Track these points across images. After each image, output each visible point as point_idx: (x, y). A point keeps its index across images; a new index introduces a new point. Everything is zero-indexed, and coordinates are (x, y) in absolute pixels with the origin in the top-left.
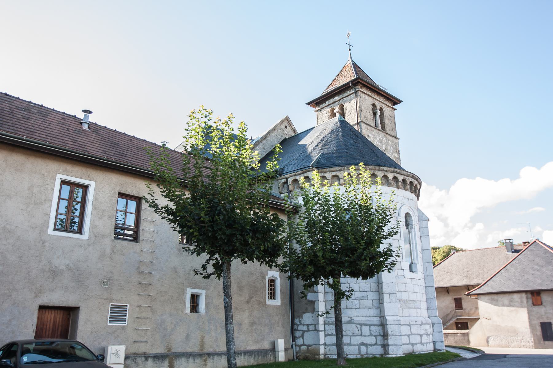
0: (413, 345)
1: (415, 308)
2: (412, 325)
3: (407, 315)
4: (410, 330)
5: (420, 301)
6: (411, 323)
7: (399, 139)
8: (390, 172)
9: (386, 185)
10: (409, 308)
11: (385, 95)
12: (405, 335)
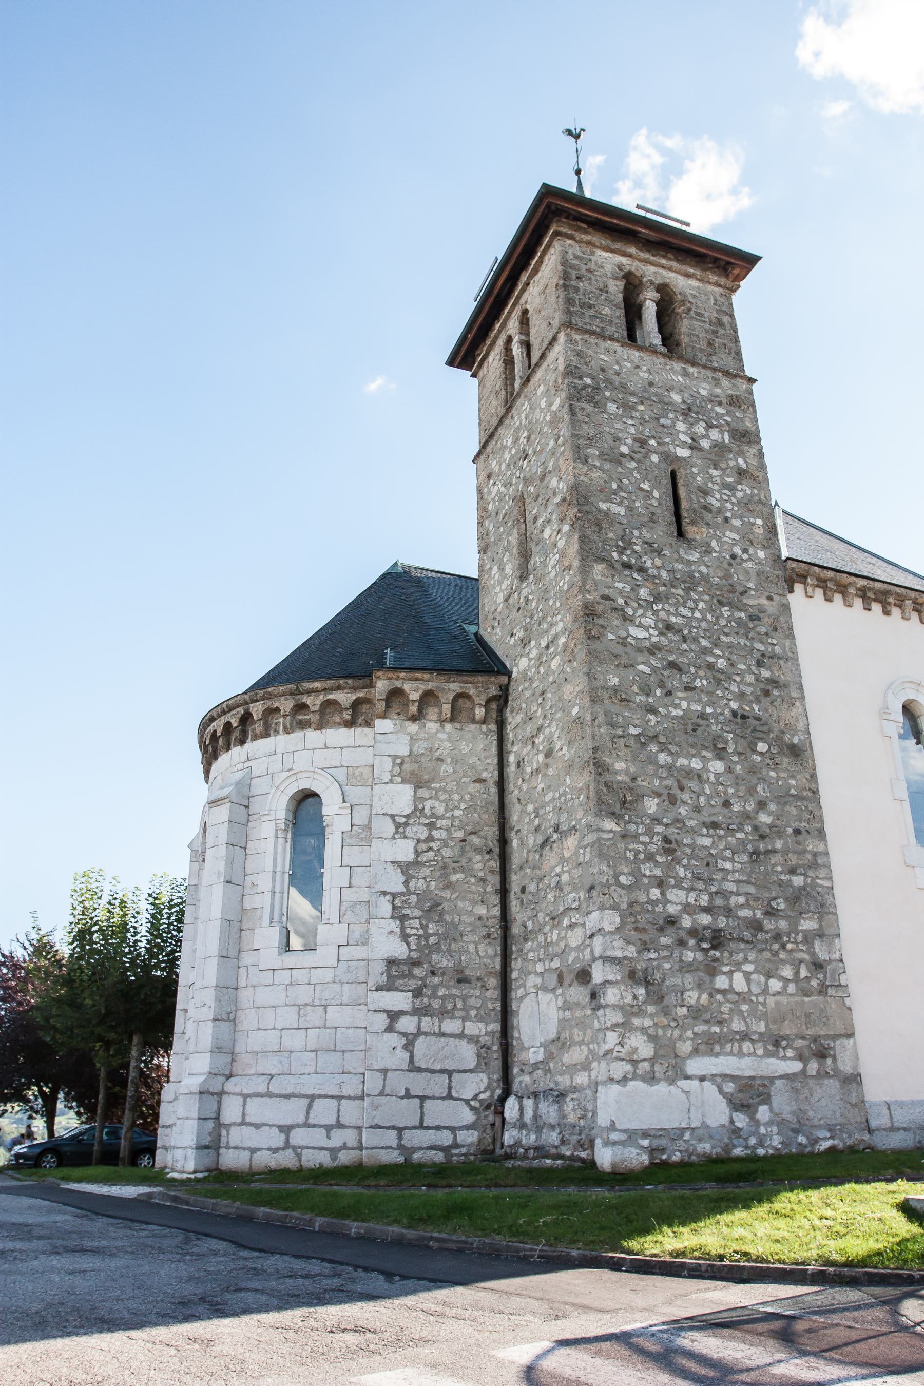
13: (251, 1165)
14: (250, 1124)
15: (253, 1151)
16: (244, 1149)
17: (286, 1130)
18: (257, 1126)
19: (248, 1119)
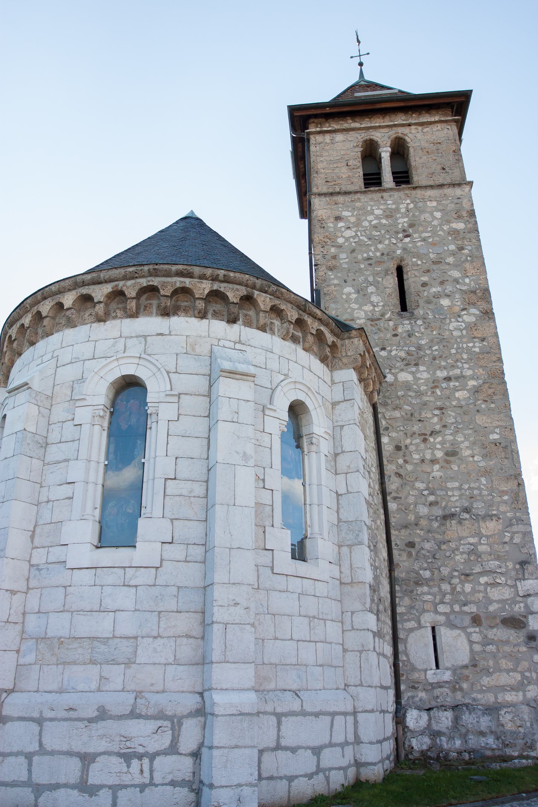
1: (93, 662)
2: (51, 720)
3: (55, 686)
4: (37, 738)
5: (136, 638)
6: (49, 714)
7: (471, 184)
8: (69, 290)
9: (67, 328)
10: (64, 663)
11: (402, 104)
13: (289, 796)
14: (286, 748)
15: (291, 779)
16: (281, 778)
17: (317, 751)
18: (294, 750)
19: (283, 743)
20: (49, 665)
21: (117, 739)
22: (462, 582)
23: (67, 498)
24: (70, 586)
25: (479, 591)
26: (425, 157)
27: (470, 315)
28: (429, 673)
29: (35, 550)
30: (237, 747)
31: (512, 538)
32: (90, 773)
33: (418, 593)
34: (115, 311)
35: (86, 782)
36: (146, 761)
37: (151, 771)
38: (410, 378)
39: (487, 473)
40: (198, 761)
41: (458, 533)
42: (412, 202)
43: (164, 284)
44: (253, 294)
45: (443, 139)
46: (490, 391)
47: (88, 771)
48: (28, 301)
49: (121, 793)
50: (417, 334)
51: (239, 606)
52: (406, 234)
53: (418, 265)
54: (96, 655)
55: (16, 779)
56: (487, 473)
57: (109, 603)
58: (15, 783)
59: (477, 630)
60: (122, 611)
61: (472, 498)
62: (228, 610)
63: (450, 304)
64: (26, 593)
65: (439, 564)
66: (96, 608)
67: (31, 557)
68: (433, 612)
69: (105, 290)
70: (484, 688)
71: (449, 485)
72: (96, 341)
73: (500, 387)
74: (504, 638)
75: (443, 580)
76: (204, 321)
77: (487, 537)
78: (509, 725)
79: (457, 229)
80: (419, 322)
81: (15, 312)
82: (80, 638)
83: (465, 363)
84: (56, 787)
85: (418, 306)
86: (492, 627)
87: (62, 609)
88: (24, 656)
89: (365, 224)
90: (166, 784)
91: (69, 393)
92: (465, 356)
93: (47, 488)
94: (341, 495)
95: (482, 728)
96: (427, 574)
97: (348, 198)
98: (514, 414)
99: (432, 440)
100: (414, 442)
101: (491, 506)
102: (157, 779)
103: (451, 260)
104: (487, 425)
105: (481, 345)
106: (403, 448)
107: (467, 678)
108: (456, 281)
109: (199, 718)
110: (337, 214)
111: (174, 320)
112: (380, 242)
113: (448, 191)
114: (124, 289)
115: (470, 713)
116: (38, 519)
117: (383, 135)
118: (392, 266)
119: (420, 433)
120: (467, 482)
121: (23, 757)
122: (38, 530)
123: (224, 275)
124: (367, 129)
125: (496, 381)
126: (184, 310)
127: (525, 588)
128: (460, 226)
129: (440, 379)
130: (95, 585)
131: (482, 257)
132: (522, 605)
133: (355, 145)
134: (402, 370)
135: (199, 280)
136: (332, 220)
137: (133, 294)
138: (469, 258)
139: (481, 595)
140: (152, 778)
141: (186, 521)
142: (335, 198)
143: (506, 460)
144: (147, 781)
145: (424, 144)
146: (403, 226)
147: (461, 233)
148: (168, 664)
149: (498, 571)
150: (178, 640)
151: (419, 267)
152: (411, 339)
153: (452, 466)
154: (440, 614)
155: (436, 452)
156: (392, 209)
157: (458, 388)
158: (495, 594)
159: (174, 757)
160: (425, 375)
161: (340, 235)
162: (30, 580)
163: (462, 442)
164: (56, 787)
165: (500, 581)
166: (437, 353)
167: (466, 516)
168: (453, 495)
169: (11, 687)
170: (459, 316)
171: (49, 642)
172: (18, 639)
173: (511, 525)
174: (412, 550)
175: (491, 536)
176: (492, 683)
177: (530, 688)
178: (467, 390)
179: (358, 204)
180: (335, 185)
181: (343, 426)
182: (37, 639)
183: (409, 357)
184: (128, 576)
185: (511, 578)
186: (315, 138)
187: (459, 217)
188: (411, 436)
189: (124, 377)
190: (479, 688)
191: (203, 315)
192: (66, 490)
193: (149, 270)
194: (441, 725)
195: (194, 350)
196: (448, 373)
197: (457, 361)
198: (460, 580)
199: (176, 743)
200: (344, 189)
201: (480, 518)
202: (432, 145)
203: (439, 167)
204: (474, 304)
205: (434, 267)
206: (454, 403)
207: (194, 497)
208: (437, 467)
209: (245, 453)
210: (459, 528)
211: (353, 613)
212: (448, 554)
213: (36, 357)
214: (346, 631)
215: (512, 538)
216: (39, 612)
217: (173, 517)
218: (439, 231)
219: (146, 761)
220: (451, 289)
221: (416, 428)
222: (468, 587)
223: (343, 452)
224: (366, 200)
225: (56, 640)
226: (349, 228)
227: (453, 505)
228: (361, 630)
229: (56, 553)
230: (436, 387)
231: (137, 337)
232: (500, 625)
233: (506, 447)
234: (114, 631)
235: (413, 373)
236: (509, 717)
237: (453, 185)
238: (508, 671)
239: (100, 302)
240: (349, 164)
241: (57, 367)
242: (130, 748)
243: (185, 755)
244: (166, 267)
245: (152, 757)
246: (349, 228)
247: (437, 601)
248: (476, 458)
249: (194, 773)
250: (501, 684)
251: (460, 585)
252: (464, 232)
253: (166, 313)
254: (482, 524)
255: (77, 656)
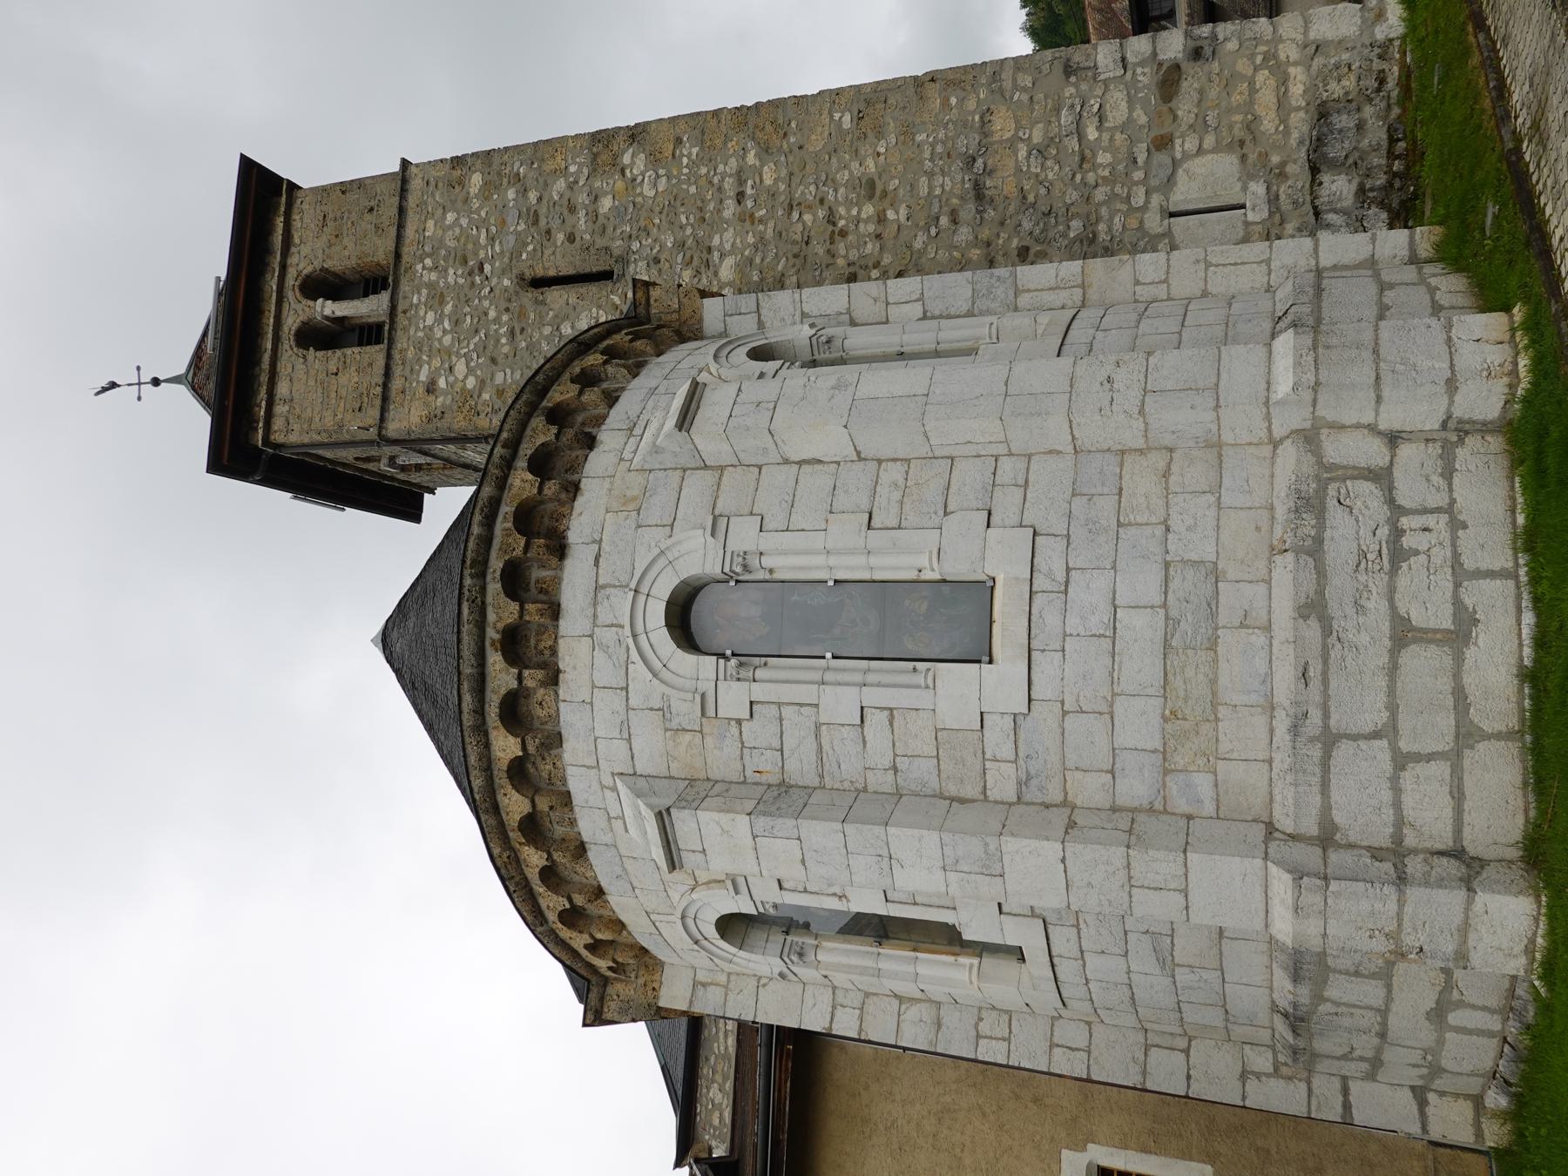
0: (1466, 735)
1: (1213, 645)
2: (1326, 715)
4: (1363, 744)
5: (1167, 565)
7: (405, 164)
8: (487, 745)
9: (560, 757)
10: (1214, 705)
12: (1397, 790)
20: (1217, 740)
21: (1362, 578)
22: (1095, 167)
23: (891, 724)
24: (1063, 703)
25: (1111, 139)
26: (346, 241)
27: (633, 163)
28: (1251, 217)
29: (989, 793)
30: (1376, 352)
31: (1024, 89)
32: (1432, 625)
33: (1109, 238)
34: (542, 653)
35: (1449, 631)
36: (1405, 522)
37: (1425, 511)
38: (729, 262)
39: (907, 132)
40: (1403, 435)
41: (1009, 176)
42: (422, 261)
43: (503, 550)
44: (546, 408)
45: (318, 211)
46: (769, 128)
47: (1426, 631)
48: (496, 851)
49: (1469, 564)
50: (655, 251)
51: (1112, 375)
52: (476, 271)
53: (534, 250)
54: (1199, 638)
55: (1447, 789)
56: (907, 132)
57: (1098, 620)
58: (1455, 790)
59: (1178, 142)
60: (1114, 592)
61: (949, 156)
62: (1119, 391)
63: (610, 197)
64: (1074, 807)
65: (1060, 205)
66: (1106, 644)
67: (1002, 803)
68: (1144, 213)
69: (497, 667)
70: (1281, 128)
71: (924, 191)
72: (594, 687)
73: (763, 112)
74: (1195, 96)
75: (1088, 199)
76: (582, 485)
77: (1017, 130)
78: (1348, 83)
79: (481, 186)
80: (635, 246)
81: (515, 895)
82: (1166, 674)
83: (715, 170)
84: (1459, 694)
85: (606, 248)
86: (1175, 117)
87: (1107, 717)
88: (1200, 801)
89: (447, 340)
90: (1450, 485)
91: (688, 737)
92: (704, 170)
93: (870, 774)
94: (925, 312)
95: (1352, 125)
96: (1076, 224)
97: (397, 370)
98: (811, 89)
99: (842, 223)
100: (843, 252)
101: (965, 126)
102: (1440, 500)
103: (533, 196)
104: (827, 133)
105: (687, 145)
106: (852, 269)
107: (1265, 156)
108: (571, 187)
109: (1323, 437)
110: (421, 390)
111: (572, 537)
112: (486, 314)
113: (412, 200)
114: (500, 626)
115: (1325, 145)
116: (929, 792)
117: (292, 312)
118: (530, 295)
119: (828, 243)
120: (921, 163)
121: (1402, 774)
122: (952, 789)
123: (503, 447)
124: (277, 339)
125: (752, 120)
126: (557, 521)
127: (1111, 66)
128: (476, 180)
129: (739, 209)
130: (1063, 651)
131: (536, 144)
132: (1139, 70)
133: (301, 360)
134: (716, 274)
135: (506, 491)
136: (431, 398)
137: (514, 607)
138: (535, 166)
139: (1118, 136)
140: (1438, 510)
141: (951, 490)
142: (393, 394)
143: (889, 102)
144: (1444, 518)
145: (321, 243)
146: (462, 276)
147: (489, 178)
148: (1219, 503)
149: (1078, 110)
150: (1172, 488)
151: (538, 248)
152: (662, 260)
153: (891, 188)
154: (1147, 202)
155: (864, 216)
156: (428, 294)
157: (758, 181)
158: (1118, 110)
159: (1397, 473)
160: (729, 235)
161: (460, 385)
162: (1048, 800)
163: (851, 173)
164: (1459, 694)
165: (1097, 106)
166: (692, 217)
167: (979, 163)
168: (942, 186)
169: (1262, 826)
170: (634, 180)
171: (1171, 744)
172: (1165, 817)
173: (1002, 92)
174: (1032, 252)
175: (1017, 122)
176: (1273, 115)
177: (1282, 56)
178: (762, 166)
179: (410, 354)
180: (368, 395)
181: (803, 313)
182: (1166, 772)
183: (696, 262)
184: (1048, 585)
185: (1091, 89)
186: (276, 432)
187: (461, 182)
188: (834, 256)
189: (669, 625)
190: (1280, 136)
191: (573, 489)
192: (876, 720)
193: (472, 576)
194: (1345, 192)
195: (634, 499)
196: (729, 197)
197: (710, 182)
198: (1090, 170)
199: (1370, 471)
200: (380, 380)
201: (984, 141)
202: (325, 228)
203: (368, 217)
204: (616, 157)
205: (543, 222)
206: (782, 187)
207: (906, 479)
208: (891, 215)
209: (833, 388)
210: (999, 174)
211: (1137, 283)
212: (1043, 191)
213: (608, 839)
214: (1169, 294)
215: (1024, 89)
216: (1112, 772)
217: (941, 513)
218: (479, 215)
219: (1405, 522)
220: (585, 195)
221: (820, 250)
222: (1103, 158)
223: (849, 312)
224: (405, 340)
225: (1168, 727)
226: (451, 368)
227: (959, 186)
228: (1169, 266)
229: (998, 739)
230: (752, 215)
231: (595, 605)
232: (1173, 104)
233: (868, 102)
234: (1152, 607)
235: (722, 256)
236: (1333, 86)
237: (403, 192)
238: (1253, 91)
239: (520, 678)
240: (335, 371)
241: (635, 774)
242: (1380, 551)
243: (1392, 457)
244: (471, 545)
245: (1397, 510)
246: (451, 368)
247: (1124, 207)
248: (882, 150)
249: (1427, 440)
250: (1275, 100)
251: (1100, 171)
252: (489, 173)
253: (559, 549)
254: (996, 137)
255: (1201, 677)
